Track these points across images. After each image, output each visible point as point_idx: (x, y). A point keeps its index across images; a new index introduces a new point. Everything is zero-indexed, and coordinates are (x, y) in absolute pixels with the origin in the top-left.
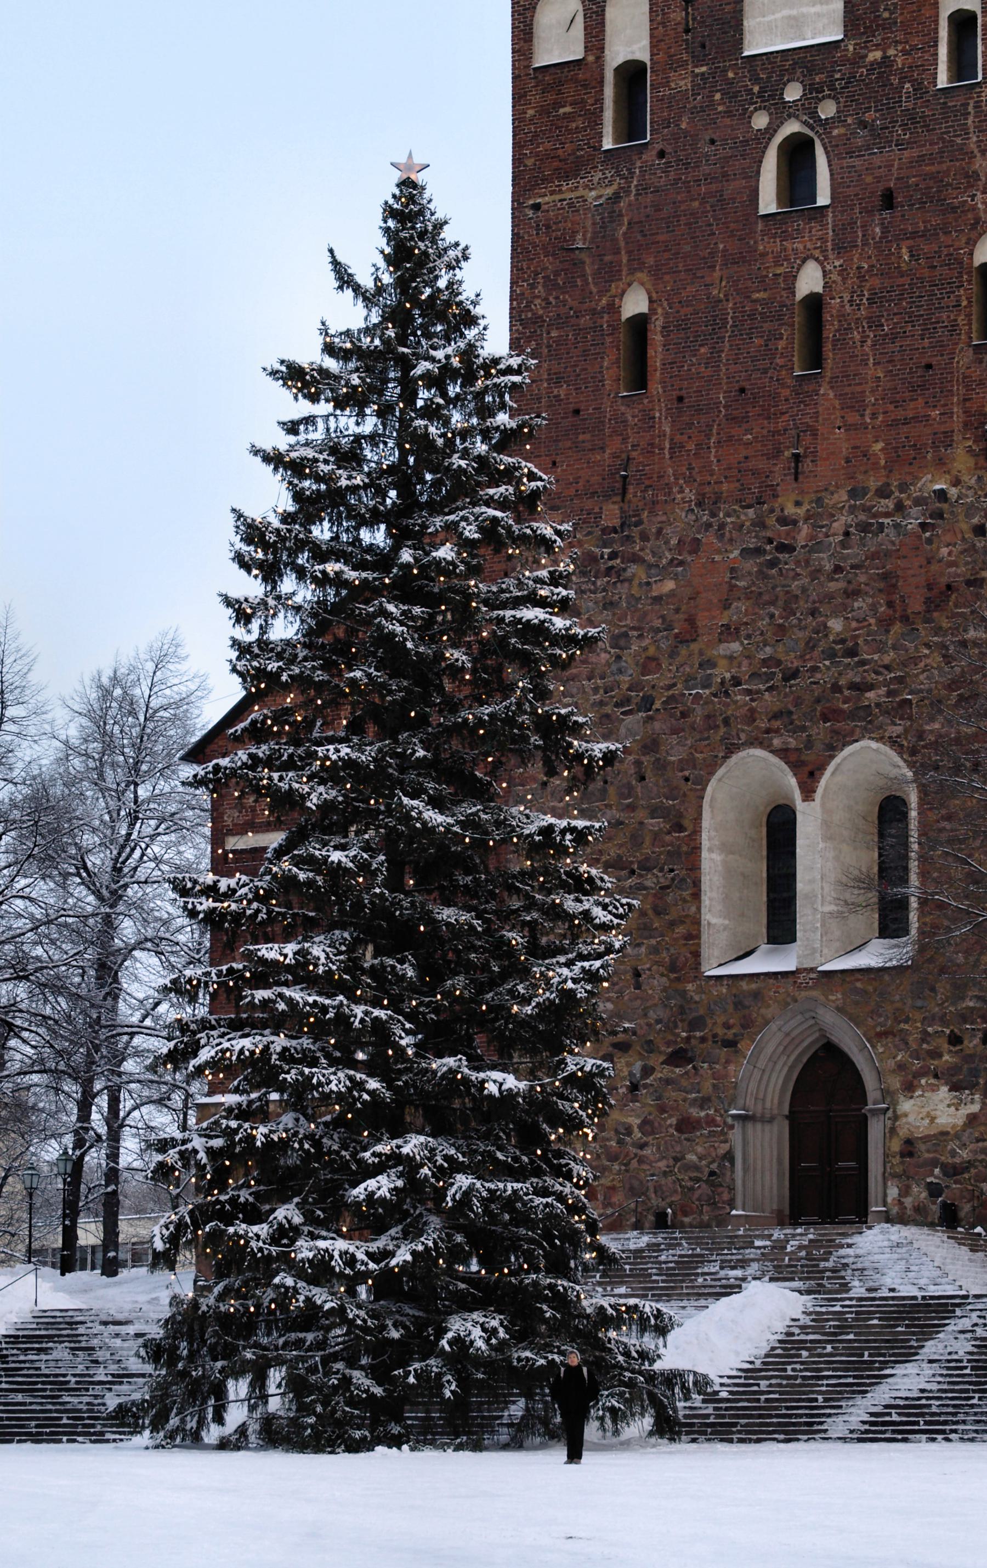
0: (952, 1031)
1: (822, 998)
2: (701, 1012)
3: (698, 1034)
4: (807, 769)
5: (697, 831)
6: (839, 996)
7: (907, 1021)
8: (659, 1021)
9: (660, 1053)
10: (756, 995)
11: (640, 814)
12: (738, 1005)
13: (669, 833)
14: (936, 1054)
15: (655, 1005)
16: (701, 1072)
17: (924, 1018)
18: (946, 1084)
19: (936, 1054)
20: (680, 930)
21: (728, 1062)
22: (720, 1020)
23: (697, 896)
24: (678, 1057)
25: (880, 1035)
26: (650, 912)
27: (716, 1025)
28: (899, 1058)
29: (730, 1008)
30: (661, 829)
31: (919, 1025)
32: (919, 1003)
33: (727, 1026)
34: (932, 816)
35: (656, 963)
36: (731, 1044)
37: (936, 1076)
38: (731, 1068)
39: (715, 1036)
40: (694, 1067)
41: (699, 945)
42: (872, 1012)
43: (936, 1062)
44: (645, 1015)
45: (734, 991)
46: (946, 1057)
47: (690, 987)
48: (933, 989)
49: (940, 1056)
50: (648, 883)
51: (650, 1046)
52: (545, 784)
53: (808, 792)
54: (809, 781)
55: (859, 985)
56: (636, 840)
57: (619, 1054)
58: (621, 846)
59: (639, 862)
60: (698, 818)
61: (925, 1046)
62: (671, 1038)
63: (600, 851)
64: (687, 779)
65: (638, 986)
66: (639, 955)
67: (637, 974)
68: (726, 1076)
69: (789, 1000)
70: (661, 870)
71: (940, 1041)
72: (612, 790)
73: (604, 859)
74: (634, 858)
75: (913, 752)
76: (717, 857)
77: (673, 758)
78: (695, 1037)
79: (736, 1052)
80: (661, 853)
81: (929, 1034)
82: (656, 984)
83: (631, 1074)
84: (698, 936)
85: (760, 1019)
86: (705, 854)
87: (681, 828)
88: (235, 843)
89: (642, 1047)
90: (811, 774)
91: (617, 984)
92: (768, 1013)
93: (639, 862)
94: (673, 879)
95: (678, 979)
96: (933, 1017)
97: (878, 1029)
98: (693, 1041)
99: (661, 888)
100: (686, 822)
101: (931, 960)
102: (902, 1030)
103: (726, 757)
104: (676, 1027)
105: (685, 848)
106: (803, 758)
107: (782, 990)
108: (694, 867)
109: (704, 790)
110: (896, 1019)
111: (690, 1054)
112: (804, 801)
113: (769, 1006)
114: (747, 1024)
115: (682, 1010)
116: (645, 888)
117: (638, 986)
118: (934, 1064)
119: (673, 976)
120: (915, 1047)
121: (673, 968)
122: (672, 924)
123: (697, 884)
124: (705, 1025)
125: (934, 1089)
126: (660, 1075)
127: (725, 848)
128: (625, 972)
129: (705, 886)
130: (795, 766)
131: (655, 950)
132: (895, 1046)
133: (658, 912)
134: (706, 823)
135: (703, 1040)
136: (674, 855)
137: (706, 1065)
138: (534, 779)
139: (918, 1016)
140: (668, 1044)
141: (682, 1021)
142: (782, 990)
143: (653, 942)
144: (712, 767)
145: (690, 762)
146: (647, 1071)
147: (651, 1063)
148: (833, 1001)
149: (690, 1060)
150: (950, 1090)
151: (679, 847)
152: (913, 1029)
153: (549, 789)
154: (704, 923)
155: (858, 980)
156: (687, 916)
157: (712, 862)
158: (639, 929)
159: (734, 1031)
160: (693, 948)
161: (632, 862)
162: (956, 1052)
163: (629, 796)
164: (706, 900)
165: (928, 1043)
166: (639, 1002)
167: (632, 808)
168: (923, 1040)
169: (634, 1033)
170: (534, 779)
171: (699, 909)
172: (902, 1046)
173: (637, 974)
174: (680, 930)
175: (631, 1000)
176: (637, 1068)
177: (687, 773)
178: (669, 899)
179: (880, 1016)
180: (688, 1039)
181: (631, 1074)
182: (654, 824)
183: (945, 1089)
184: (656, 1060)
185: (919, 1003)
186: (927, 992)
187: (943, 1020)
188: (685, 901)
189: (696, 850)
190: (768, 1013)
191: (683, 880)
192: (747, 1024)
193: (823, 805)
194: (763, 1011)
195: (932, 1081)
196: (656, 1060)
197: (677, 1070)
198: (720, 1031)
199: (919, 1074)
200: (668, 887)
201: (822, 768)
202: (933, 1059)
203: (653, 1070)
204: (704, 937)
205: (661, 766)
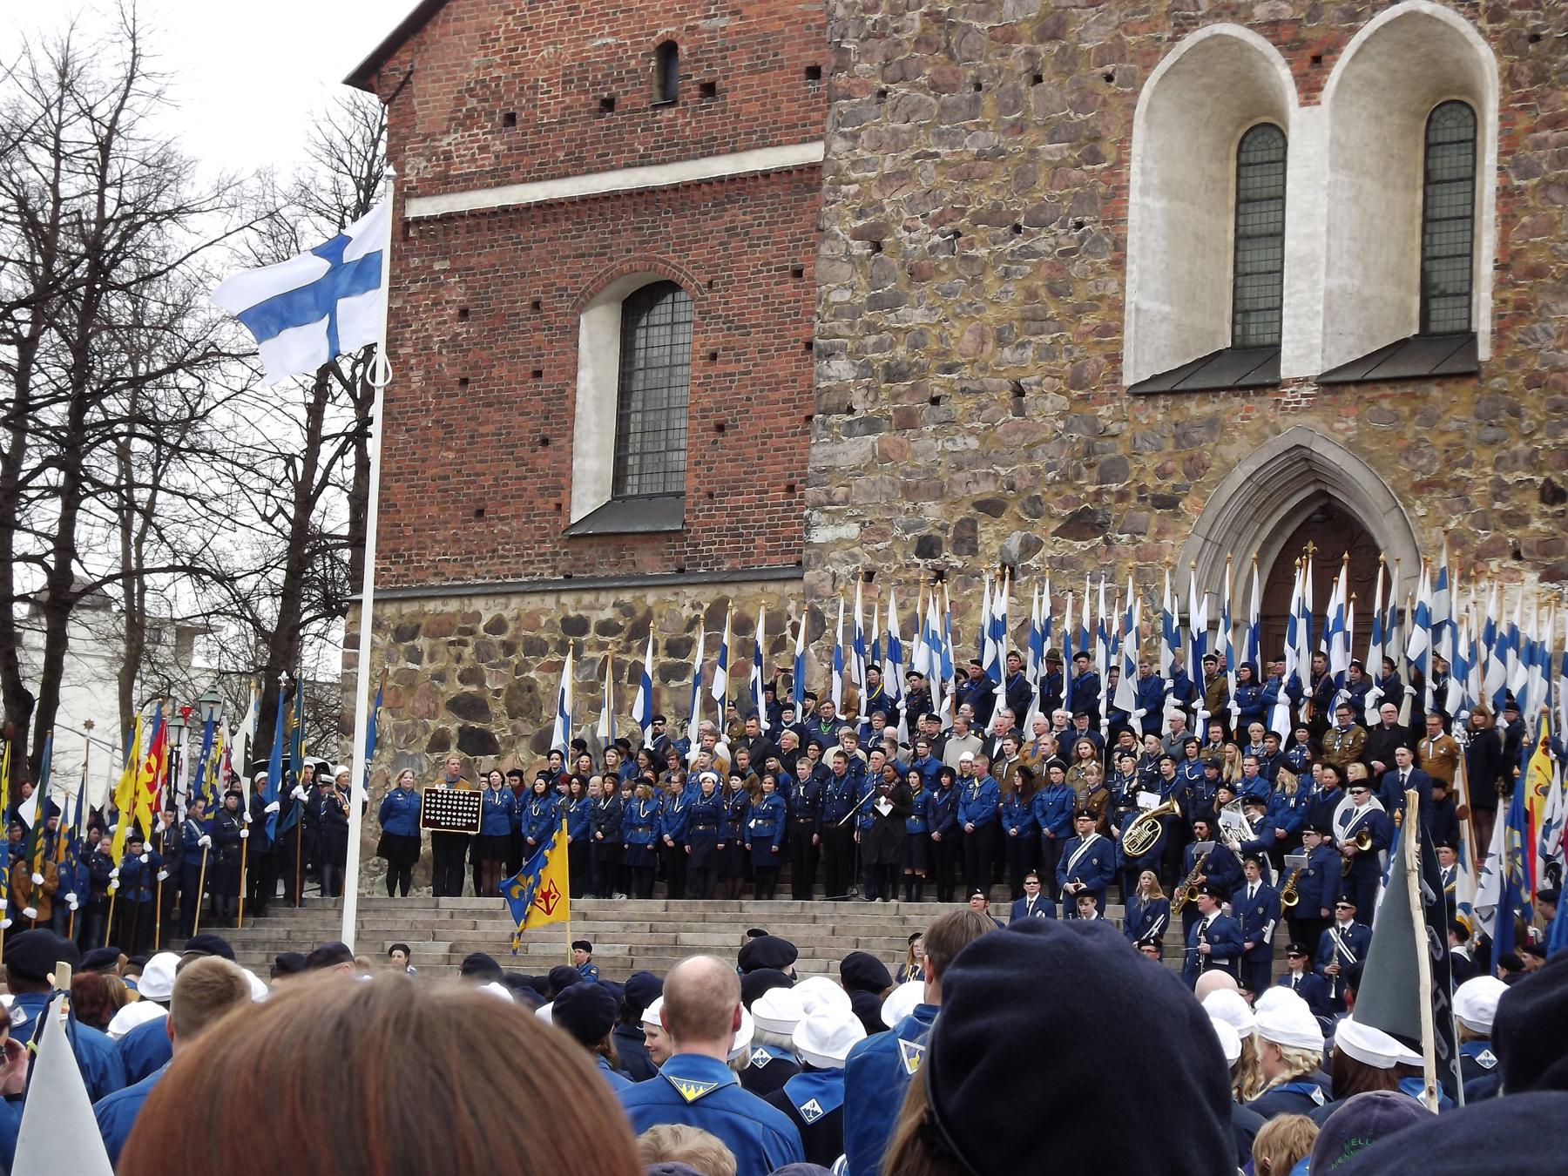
0: (1548, 481)
1: (1323, 427)
2: (1121, 451)
3: (1114, 487)
4: (1308, 54)
5: (1122, 161)
6: (1352, 423)
7: (1467, 464)
8: (1050, 468)
9: (1052, 517)
10: (1213, 425)
11: (1031, 137)
12: (1182, 438)
13: (1077, 165)
14: (1517, 519)
15: (1046, 441)
16: (1118, 547)
17: (1499, 460)
18: (1535, 568)
19: (1517, 519)
20: (1091, 320)
21: (1161, 532)
22: (1152, 462)
23: (1119, 264)
24: (1081, 524)
25: (1421, 488)
26: (1043, 292)
27: (1146, 470)
28: (1452, 525)
29: (1169, 446)
30: (1064, 159)
31: (1488, 470)
32: (1491, 433)
33: (1163, 474)
34: (1524, 121)
35: (1050, 374)
36: (1168, 503)
37: (1517, 556)
38: (1168, 541)
39: (1141, 489)
40: (1106, 540)
41: (1120, 343)
42: (1408, 449)
43: (1517, 533)
44: (1030, 458)
45: (1175, 417)
46: (1536, 523)
47: (1103, 411)
48: (1515, 412)
49: (1525, 521)
50: (1041, 246)
51: (1035, 507)
52: (883, 93)
53: (1309, 90)
54: (1312, 72)
55: (1386, 404)
56: (1023, 180)
57: (987, 519)
58: (998, 188)
59: (1028, 213)
60: (1124, 142)
61: (1498, 505)
62: (1070, 493)
63: (966, 197)
64: (1109, 78)
65: (1019, 411)
66: (1022, 361)
67: (1019, 392)
68: (1159, 554)
69: (1267, 430)
70: (1063, 225)
71: (1527, 496)
72: (987, 101)
73: (971, 209)
74: (1019, 207)
75: (1496, 15)
76: (1157, 204)
77: (1088, 46)
78: (1109, 492)
79: (1177, 515)
80: (1063, 198)
81: (1506, 486)
82: (1048, 406)
83: (1003, 550)
84: (1119, 330)
85: (1216, 463)
86: (1134, 197)
87: (1095, 157)
88: (419, 208)
89: (1023, 507)
90: (1317, 60)
91: (986, 407)
92: (1230, 452)
93: (1028, 213)
94: (1081, 239)
95: (1084, 398)
96: (1515, 457)
97: (1418, 477)
98: (1106, 499)
99: (1062, 253)
100: (1106, 148)
101: (1513, 363)
102: (1458, 479)
103: (1174, 39)
104: (1078, 476)
105: (1102, 189)
106: (1304, 34)
107: (1254, 415)
108: (1115, 218)
109: (1136, 94)
110: (1448, 461)
111: (1100, 519)
112: (1302, 105)
113: (1233, 441)
114: (1196, 469)
115: (1089, 452)
116: (1036, 254)
117: (1019, 411)
118: (1512, 535)
119: (1075, 393)
120: (1480, 507)
121: (1076, 381)
122: (1079, 310)
123: (1119, 245)
124: (1127, 473)
125: (1513, 576)
126: (1050, 553)
127: (1171, 190)
128: (1000, 388)
129: (1132, 250)
130: (1291, 48)
131: (1048, 353)
132: (1446, 506)
133: (1055, 293)
134: (1137, 148)
135: (1122, 496)
136: (1086, 199)
137: (1125, 537)
138: (866, 88)
139: (1488, 455)
140: (1066, 503)
141: (1090, 466)
142: (1254, 415)
143: (1047, 339)
144: (1149, 58)
145: (1115, 51)
146: (1030, 547)
147: (1036, 534)
148: (1341, 432)
149: (1101, 528)
150: (1541, 580)
151: (1093, 186)
152: (1480, 479)
153: (889, 103)
154: (1129, 307)
155: (1384, 396)
156: (1101, 298)
157: (1145, 212)
158: (1023, 320)
159: (1171, 482)
160: (1110, 349)
161: (1016, 214)
162: (1555, 516)
163: (1016, 108)
164: (1132, 267)
165: (1504, 500)
166: (1020, 436)
167: (1019, 128)
168: (1496, 496)
169: (1012, 487)
170: (866, 88)
171: (1122, 285)
172: (1457, 506)
173: (1019, 392)
174: (1091, 320)
175: (1006, 432)
176: (1014, 543)
177: (1109, 68)
178: (1074, 271)
179: (1421, 455)
180: (1098, 494)
181: (1003, 550)
182: (1053, 151)
183: (1532, 577)
184: (1043, 529)
185: (1491, 433)
186: (1504, 417)
187: (1532, 462)
188: (1100, 273)
189: (1119, 192)
190: (1230, 452)
191: (1098, 240)
192: (1196, 469)
193: (1335, 109)
194: (1222, 449)
195: (1513, 563)
196: (1043, 529)
197: (1078, 545)
198: (1150, 482)
199: (1483, 555)
200: (1073, 251)
201: (1335, 48)
202: (1513, 527)
203: (1039, 544)
204: (1129, 331)
205: (1069, 60)
